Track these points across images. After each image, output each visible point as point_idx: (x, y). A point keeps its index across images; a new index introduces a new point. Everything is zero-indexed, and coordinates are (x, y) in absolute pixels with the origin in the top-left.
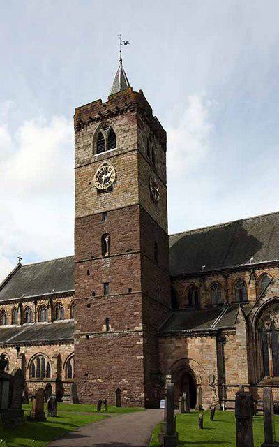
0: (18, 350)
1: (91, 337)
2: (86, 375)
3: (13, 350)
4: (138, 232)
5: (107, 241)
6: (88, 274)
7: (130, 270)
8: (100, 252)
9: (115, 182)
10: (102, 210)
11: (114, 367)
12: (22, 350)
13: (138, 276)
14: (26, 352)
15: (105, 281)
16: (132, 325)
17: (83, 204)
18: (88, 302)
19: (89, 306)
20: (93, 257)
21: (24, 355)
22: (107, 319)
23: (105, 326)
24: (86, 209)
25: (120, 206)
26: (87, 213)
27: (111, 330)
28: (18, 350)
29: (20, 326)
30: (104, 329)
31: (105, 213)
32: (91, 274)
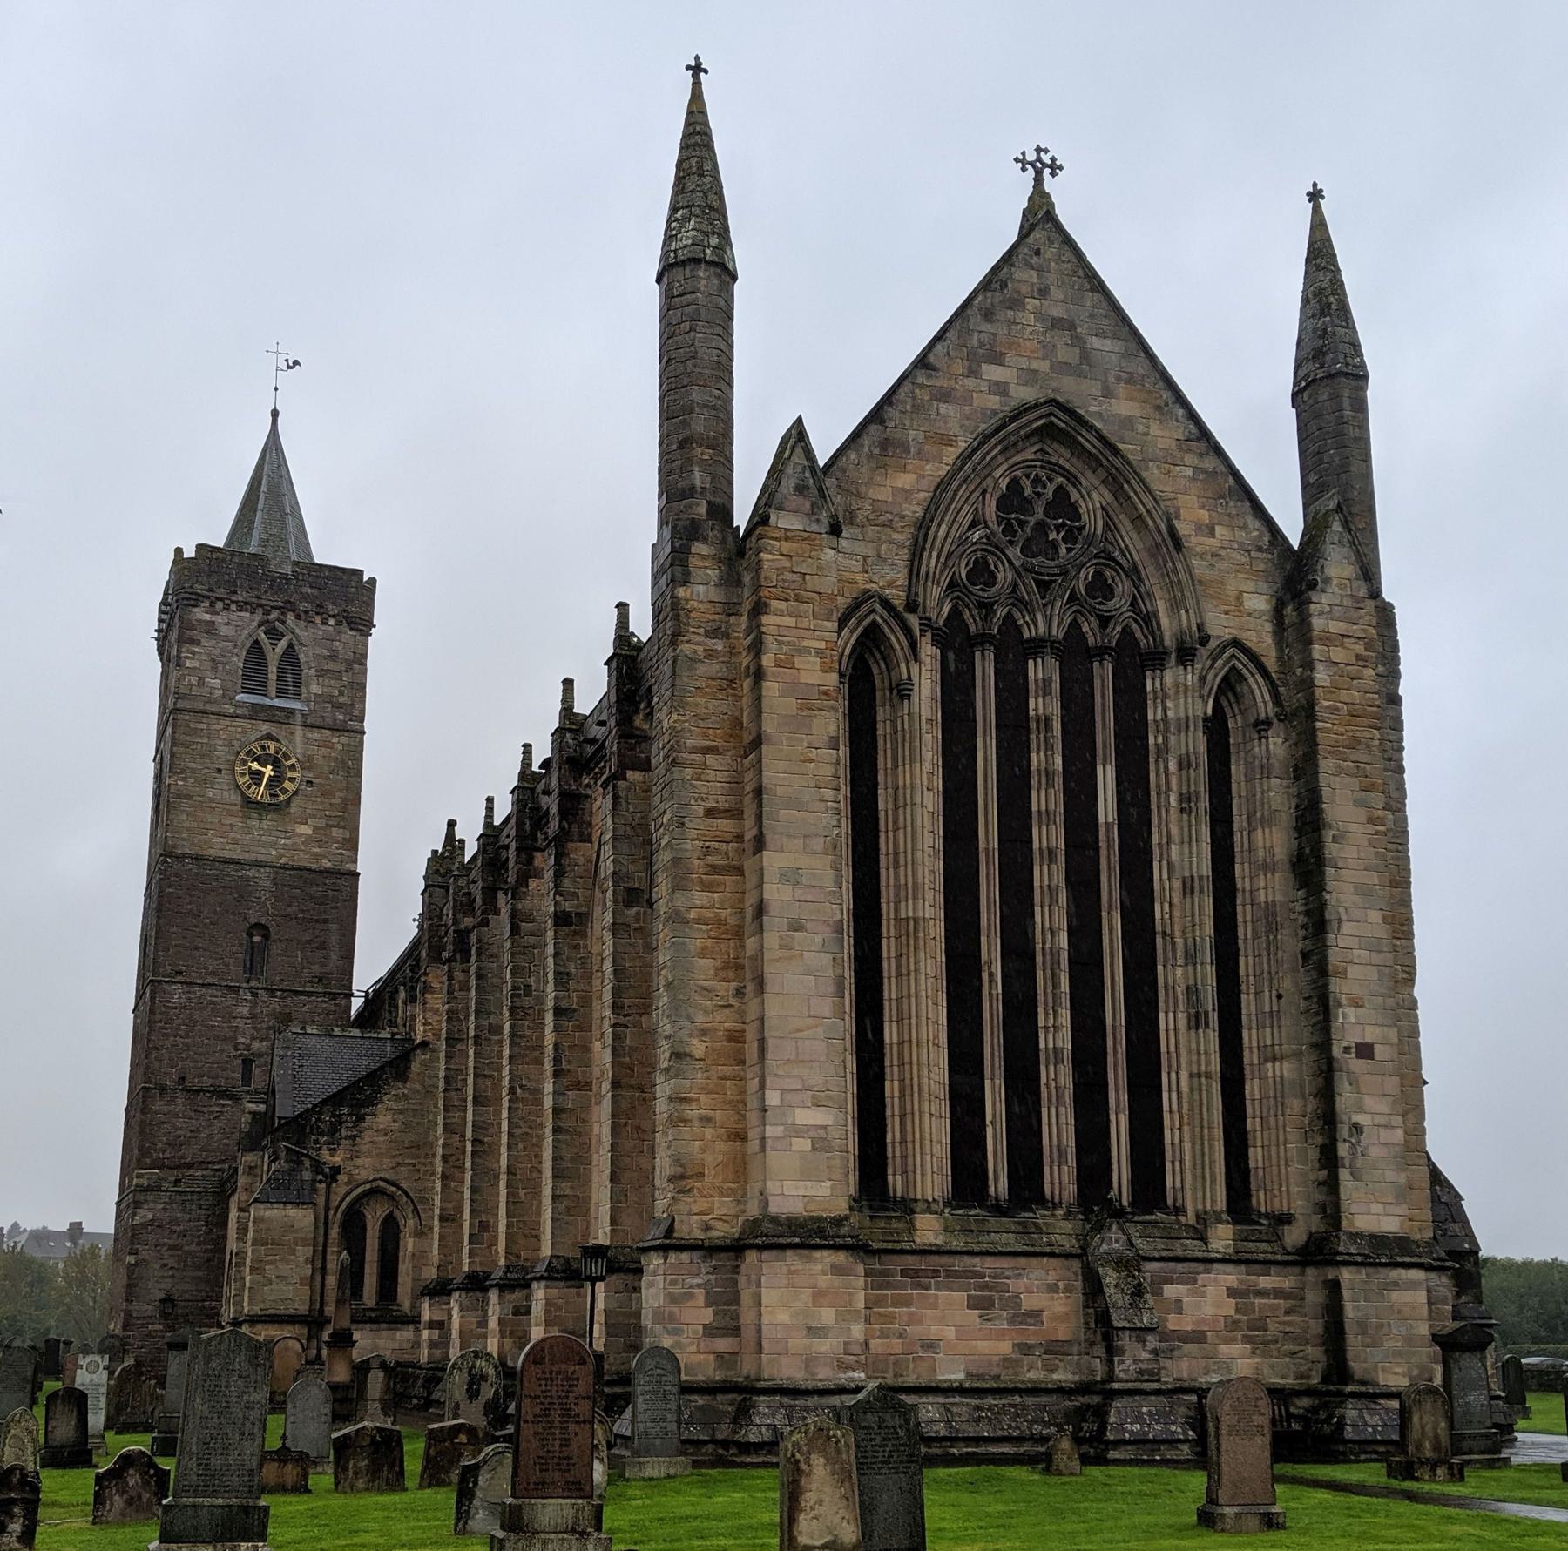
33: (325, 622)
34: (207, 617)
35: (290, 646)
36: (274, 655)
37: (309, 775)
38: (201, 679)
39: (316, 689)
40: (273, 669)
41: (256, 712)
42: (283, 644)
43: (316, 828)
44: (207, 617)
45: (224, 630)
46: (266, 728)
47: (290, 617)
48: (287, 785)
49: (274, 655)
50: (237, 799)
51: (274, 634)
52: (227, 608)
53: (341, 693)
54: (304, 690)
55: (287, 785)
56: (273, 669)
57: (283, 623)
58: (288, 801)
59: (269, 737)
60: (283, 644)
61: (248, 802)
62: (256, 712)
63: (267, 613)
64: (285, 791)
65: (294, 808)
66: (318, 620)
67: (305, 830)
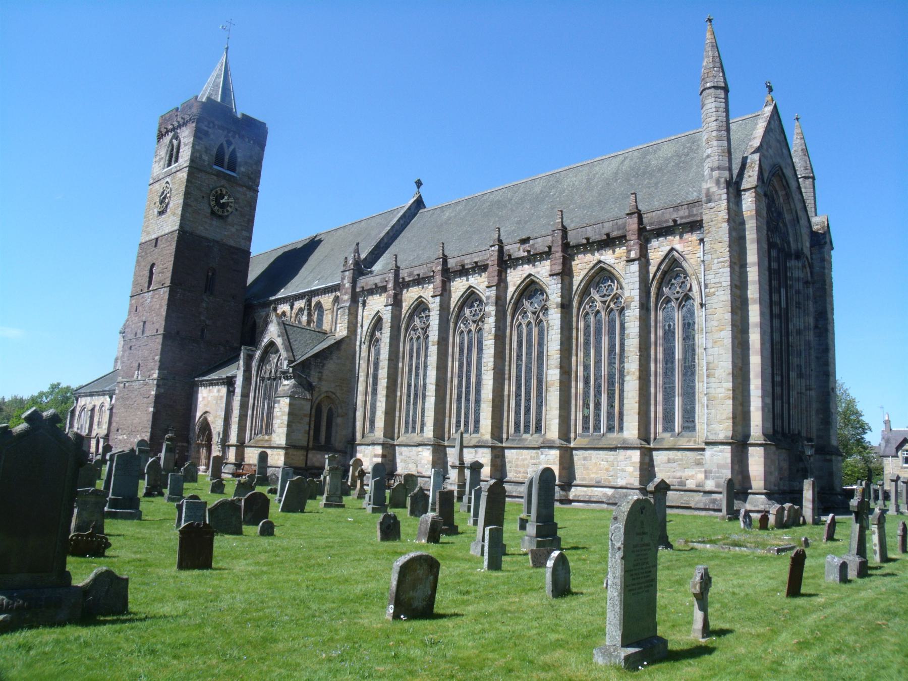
1: (127, 384)
2: (118, 430)
4: (172, 262)
7: (161, 306)
8: (146, 285)
10: (154, 236)
11: (135, 421)
13: (164, 314)
15: (144, 319)
19: (131, 347)
22: (139, 364)
23: (136, 372)
25: (167, 231)
27: (139, 378)
30: (135, 377)
31: (157, 239)
32: (140, 309)
33: (249, 142)
35: (234, 150)
37: (237, 206)
38: (201, 156)
39: (243, 169)
41: (219, 174)
42: (232, 148)
43: (237, 230)
44: (206, 128)
45: (212, 136)
46: (223, 182)
47: (237, 136)
48: (229, 208)
50: (209, 211)
51: (229, 143)
54: (237, 168)
55: (229, 208)
57: (234, 137)
58: (227, 216)
59: (223, 186)
60: (232, 148)
62: (219, 174)
63: (228, 132)
64: (228, 211)
65: (230, 219)
66: (247, 140)
67: (234, 230)
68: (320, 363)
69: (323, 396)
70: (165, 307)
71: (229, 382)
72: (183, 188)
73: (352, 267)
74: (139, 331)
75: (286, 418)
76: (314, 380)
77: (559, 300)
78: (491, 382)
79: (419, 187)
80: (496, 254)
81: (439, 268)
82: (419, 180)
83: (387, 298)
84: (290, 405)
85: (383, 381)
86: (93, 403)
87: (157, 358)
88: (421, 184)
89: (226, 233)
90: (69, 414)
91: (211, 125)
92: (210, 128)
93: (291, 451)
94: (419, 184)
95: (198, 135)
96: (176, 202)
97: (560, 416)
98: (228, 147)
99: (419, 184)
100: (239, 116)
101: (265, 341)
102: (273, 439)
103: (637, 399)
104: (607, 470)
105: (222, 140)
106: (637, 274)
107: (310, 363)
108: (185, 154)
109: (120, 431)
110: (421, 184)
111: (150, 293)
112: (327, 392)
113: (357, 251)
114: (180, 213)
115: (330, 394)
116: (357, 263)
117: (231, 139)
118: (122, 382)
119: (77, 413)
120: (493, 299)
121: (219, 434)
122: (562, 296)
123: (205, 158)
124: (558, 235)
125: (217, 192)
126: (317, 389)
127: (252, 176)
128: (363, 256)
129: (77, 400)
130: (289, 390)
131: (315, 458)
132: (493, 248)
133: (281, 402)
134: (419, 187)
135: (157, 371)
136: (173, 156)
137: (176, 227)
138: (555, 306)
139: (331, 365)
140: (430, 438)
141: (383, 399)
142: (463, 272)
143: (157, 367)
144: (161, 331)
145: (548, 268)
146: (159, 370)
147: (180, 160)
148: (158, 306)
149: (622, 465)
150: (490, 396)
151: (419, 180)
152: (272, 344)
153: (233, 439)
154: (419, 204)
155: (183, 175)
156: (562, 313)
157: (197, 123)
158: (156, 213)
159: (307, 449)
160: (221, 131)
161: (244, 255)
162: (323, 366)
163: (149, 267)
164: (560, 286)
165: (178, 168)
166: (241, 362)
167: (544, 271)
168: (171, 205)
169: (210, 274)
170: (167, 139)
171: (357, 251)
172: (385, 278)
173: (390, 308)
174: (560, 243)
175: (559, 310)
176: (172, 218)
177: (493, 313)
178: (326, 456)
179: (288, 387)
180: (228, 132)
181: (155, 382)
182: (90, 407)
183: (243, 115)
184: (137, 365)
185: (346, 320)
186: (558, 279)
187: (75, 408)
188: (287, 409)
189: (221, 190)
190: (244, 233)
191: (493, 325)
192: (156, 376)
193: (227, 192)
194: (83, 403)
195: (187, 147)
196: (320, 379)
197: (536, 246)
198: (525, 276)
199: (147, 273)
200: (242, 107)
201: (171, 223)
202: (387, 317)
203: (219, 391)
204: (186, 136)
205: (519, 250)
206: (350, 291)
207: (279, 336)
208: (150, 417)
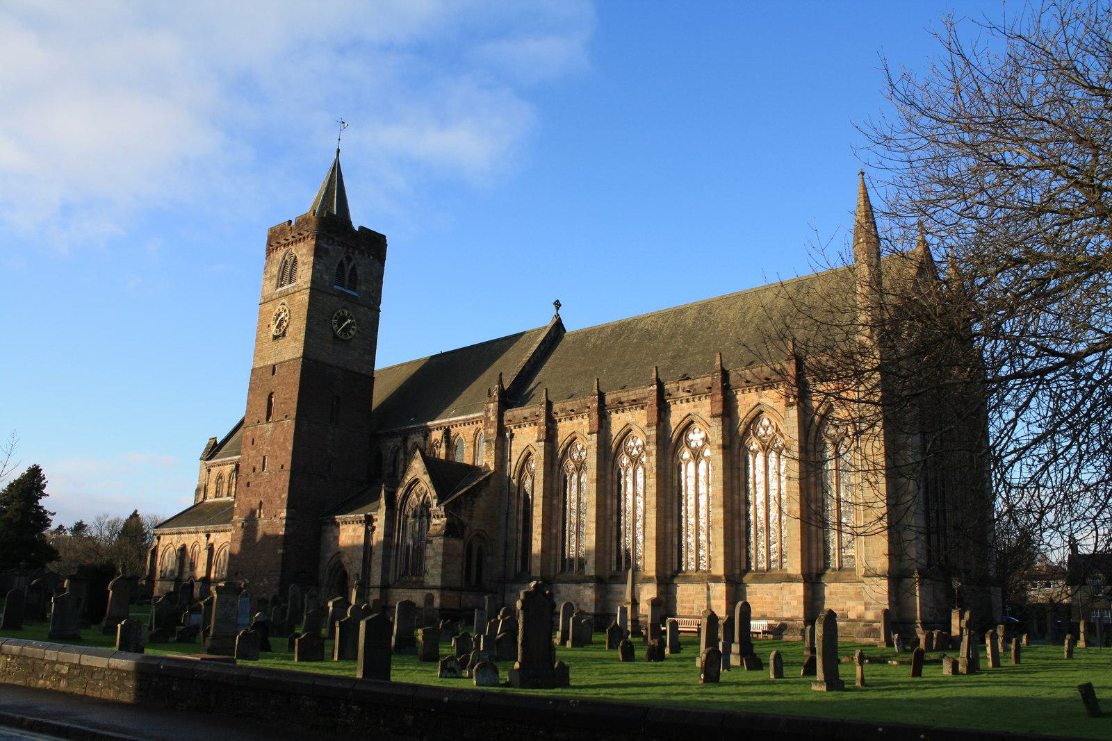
0: (208, 536)
2: (237, 574)
3: (204, 537)
5: (273, 401)
6: (253, 443)
7: (285, 440)
8: (265, 415)
9: (288, 326)
10: (273, 362)
12: (211, 540)
13: (291, 448)
14: (215, 541)
16: (279, 511)
17: (261, 351)
18: (248, 480)
19: (248, 484)
20: (259, 422)
21: (212, 545)
22: (261, 503)
23: (258, 511)
24: (262, 358)
26: (262, 365)
28: (208, 536)
29: (233, 500)
34: (326, 246)
36: (348, 268)
38: (321, 276)
39: (364, 288)
40: (347, 275)
42: (352, 264)
44: (326, 246)
47: (357, 252)
48: (351, 332)
49: (348, 268)
51: (349, 259)
52: (333, 244)
53: (373, 291)
54: (358, 288)
55: (351, 332)
56: (347, 275)
57: (353, 254)
60: (352, 264)
61: (335, 337)
63: (348, 248)
64: (350, 334)
68: (470, 501)
69: (473, 534)
70: (292, 441)
71: (369, 521)
72: (304, 312)
73: (497, 399)
74: (259, 467)
75: (440, 559)
76: (464, 519)
77: (720, 442)
78: (654, 521)
79: (558, 309)
80: (655, 393)
81: (595, 405)
82: (558, 301)
83: (540, 432)
84: (444, 545)
85: (538, 518)
86: (182, 543)
87: (285, 496)
88: (560, 305)
89: (349, 358)
90: (149, 555)
91: (331, 241)
92: (330, 245)
93: (447, 593)
94: (558, 305)
95: (318, 253)
96: (298, 328)
97: (725, 553)
98: (348, 265)
99: (558, 305)
100: (357, 229)
101: (409, 478)
102: (425, 581)
103: (799, 536)
104: (772, 603)
105: (342, 256)
106: (796, 419)
107: (461, 502)
108: (304, 275)
109: (239, 575)
110: (560, 305)
111: (270, 426)
112: (476, 530)
113: (500, 382)
114: (303, 339)
115: (481, 532)
116: (502, 393)
117: (351, 255)
118: (239, 521)
119: (160, 554)
120: (654, 439)
121: (358, 575)
122: (723, 438)
123: (326, 277)
124: (718, 376)
125: (338, 314)
126: (468, 528)
127: (373, 295)
128: (506, 387)
129: (159, 538)
130: (441, 530)
131: (469, 599)
132: (652, 388)
133: (434, 542)
134: (558, 309)
135: (285, 510)
136: (287, 273)
137: (300, 353)
138: (716, 447)
139: (481, 503)
140: (592, 576)
141: (539, 538)
142: (620, 406)
143: (285, 505)
144: (288, 466)
145: (709, 408)
146: (287, 508)
147: (299, 281)
148: (282, 440)
149: (788, 598)
150: (654, 535)
151: (558, 301)
152: (416, 481)
153: (376, 579)
154: (558, 327)
155: (304, 297)
156: (724, 454)
157: (317, 240)
158: (271, 337)
159: (459, 589)
160: (340, 248)
161: (367, 378)
162: (473, 503)
163: (267, 397)
164: (721, 428)
165: (296, 289)
166: (383, 501)
167: (704, 411)
168: (290, 329)
169: (335, 403)
170: (279, 254)
171: (500, 382)
172: (534, 413)
173: (542, 444)
174: (720, 385)
175: (721, 451)
176: (293, 344)
177: (654, 453)
178: (486, 597)
179: (440, 527)
180: (348, 248)
181: (284, 522)
182: (179, 546)
183: (361, 228)
184: (258, 502)
185: (493, 455)
186: (719, 420)
187: (156, 547)
188: (440, 550)
189: (343, 312)
190: (367, 357)
191: (654, 464)
192: (284, 514)
193: (349, 314)
194: (167, 542)
195: (306, 267)
196: (471, 518)
197: (695, 387)
198: (684, 415)
199: (265, 404)
200: (359, 218)
201: (292, 349)
202: (539, 452)
203: (354, 530)
204: (304, 253)
205: (678, 389)
206: (496, 424)
207: (425, 473)
208: (280, 559)
